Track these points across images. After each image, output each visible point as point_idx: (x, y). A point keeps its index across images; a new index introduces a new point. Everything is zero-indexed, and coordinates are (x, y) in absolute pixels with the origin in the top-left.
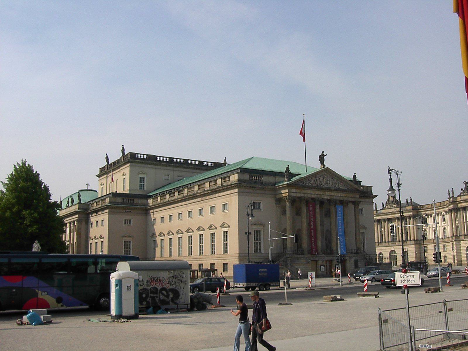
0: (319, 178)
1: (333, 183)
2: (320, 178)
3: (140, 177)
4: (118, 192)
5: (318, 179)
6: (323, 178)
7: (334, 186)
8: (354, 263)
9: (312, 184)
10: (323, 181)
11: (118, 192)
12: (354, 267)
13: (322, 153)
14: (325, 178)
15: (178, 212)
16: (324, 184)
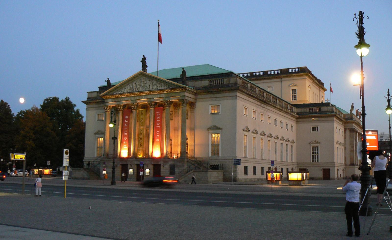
0: (136, 83)
1: (150, 86)
2: (136, 83)
3: (292, 89)
4: (323, 102)
5: (134, 85)
6: (141, 83)
7: (152, 89)
8: (169, 168)
9: (127, 91)
10: (140, 85)
11: (323, 102)
12: (169, 172)
13: (143, 57)
14: (142, 82)
15: (280, 120)
16: (142, 88)
